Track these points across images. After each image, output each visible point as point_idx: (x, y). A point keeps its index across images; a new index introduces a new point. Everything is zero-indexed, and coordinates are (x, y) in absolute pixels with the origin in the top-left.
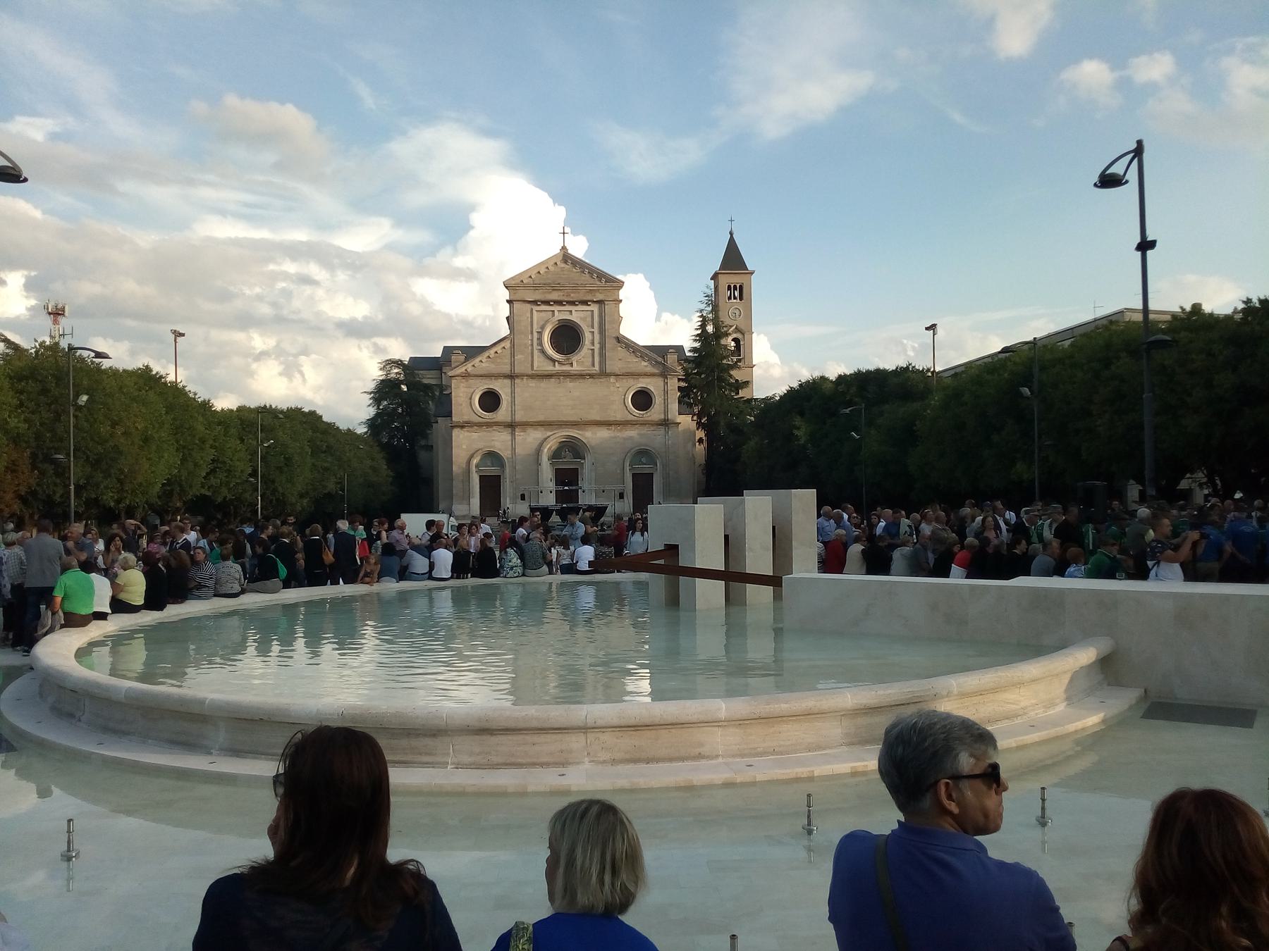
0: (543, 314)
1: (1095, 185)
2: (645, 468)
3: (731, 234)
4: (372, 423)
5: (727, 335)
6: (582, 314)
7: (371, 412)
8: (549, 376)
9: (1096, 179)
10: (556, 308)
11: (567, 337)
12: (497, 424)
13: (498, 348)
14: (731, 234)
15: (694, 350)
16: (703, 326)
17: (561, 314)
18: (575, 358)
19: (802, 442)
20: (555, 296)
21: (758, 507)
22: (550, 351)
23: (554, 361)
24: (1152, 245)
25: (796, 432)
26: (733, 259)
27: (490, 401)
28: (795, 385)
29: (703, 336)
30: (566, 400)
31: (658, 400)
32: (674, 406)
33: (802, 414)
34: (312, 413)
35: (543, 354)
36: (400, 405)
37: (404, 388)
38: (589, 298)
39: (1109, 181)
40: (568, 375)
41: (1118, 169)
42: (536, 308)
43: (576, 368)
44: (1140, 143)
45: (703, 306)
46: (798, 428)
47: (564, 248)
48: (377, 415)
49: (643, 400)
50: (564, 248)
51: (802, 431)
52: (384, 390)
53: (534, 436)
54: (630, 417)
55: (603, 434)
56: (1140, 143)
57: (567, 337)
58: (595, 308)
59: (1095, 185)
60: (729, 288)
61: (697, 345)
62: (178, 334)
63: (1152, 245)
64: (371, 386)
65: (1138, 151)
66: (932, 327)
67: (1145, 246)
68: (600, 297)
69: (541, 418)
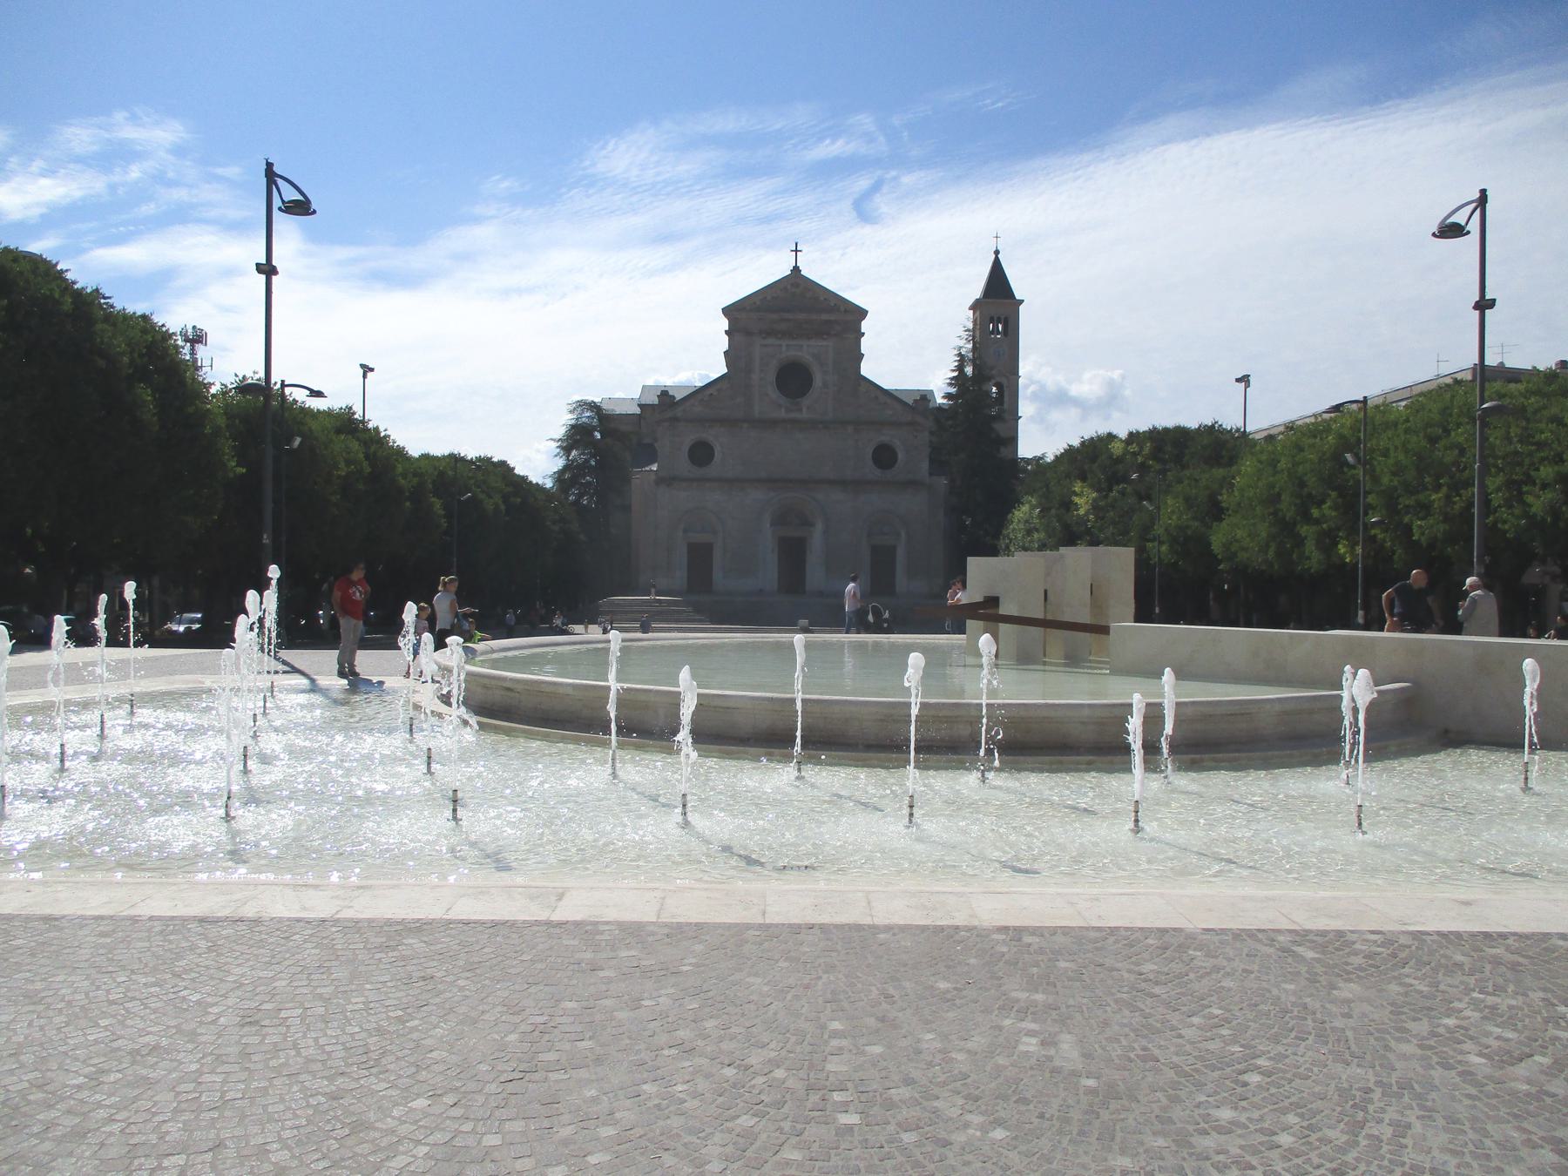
1: (1434, 235)
3: (997, 252)
4: (559, 477)
5: (989, 379)
7: (560, 463)
8: (772, 424)
9: (1435, 229)
11: (794, 379)
13: (711, 391)
14: (997, 252)
15: (948, 396)
16: (960, 368)
17: (790, 350)
18: (806, 401)
19: (1082, 512)
21: (1078, 559)
24: (1492, 304)
25: (1076, 499)
26: (998, 285)
27: (701, 453)
28: (1076, 443)
29: (959, 380)
32: (925, 465)
33: (1084, 479)
34: (503, 464)
35: (767, 398)
36: (593, 456)
37: (598, 436)
39: (1451, 230)
40: (794, 421)
41: (1460, 218)
43: (805, 415)
44: (1483, 192)
45: (962, 343)
46: (1079, 495)
47: (796, 269)
48: (566, 468)
49: (884, 456)
50: (796, 269)
51: (1084, 500)
52: (576, 437)
56: (1483, 192)
57: (794, 379)
59: (1434, 235)
61: (953, 390)
62: (367, 369)
63: (1492, 304)
64: (560, 432)
65: (1483, 199)
66: (1244, 380)
67: (1484, 305)
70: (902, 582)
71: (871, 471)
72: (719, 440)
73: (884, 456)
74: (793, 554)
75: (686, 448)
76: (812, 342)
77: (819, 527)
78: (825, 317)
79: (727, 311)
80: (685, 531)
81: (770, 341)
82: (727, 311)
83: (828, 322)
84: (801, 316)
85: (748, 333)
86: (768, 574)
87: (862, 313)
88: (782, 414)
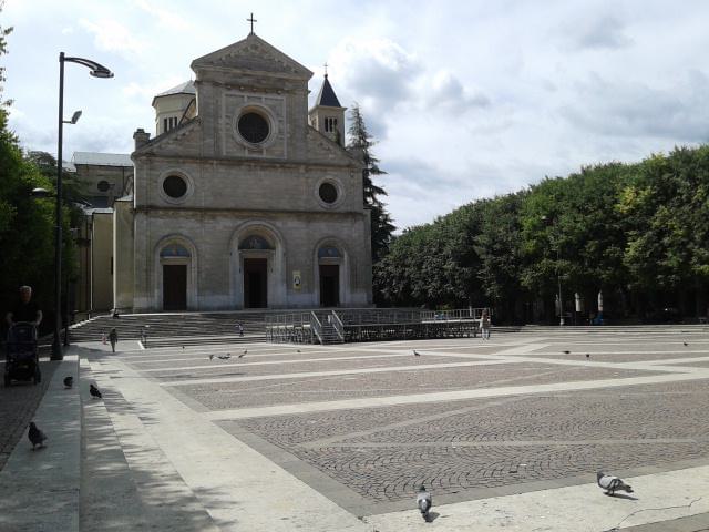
0: (231, 99)
2: (331, 261)
3: (326, 76)
6: (270, 103)
10: (246, 94)
11: (253, 127)
12: (184, 209)
14: (326, 76)
18: (264, 145)
20: (245, 80)
22: (239, 138)
23: (245, 148)
27: (175, 186)
30: (255, 187)
31: (341, 193)
35: (231, 141)
38: (279, 85)
42: (225, 92)
43: (265, 156)
47: (252, 34)
49: (328, 192)
50: (252, 34)
53: (224, 224)
54: (319, 209)
55: (293, 224)
58: (284, 97)
60: (326, 120)
68: (289, 86)
69: (231, 205)
70: (345, 293)
71: (318, 204)
72: (191, 175)
73: (328, 192)
74: (255, 278)
75: (161, 180)
76: (269, 96)
77: (280, 249)
78: (279, 75)
79: (196, 65)
80: (162, 255)
81: (233, 92)
82: (196, 65)
83: (280, 79)
84: (260, 73)
85: (216, 84)
86: (236, 293)
87: (312, 74)
88: (247, 154)
